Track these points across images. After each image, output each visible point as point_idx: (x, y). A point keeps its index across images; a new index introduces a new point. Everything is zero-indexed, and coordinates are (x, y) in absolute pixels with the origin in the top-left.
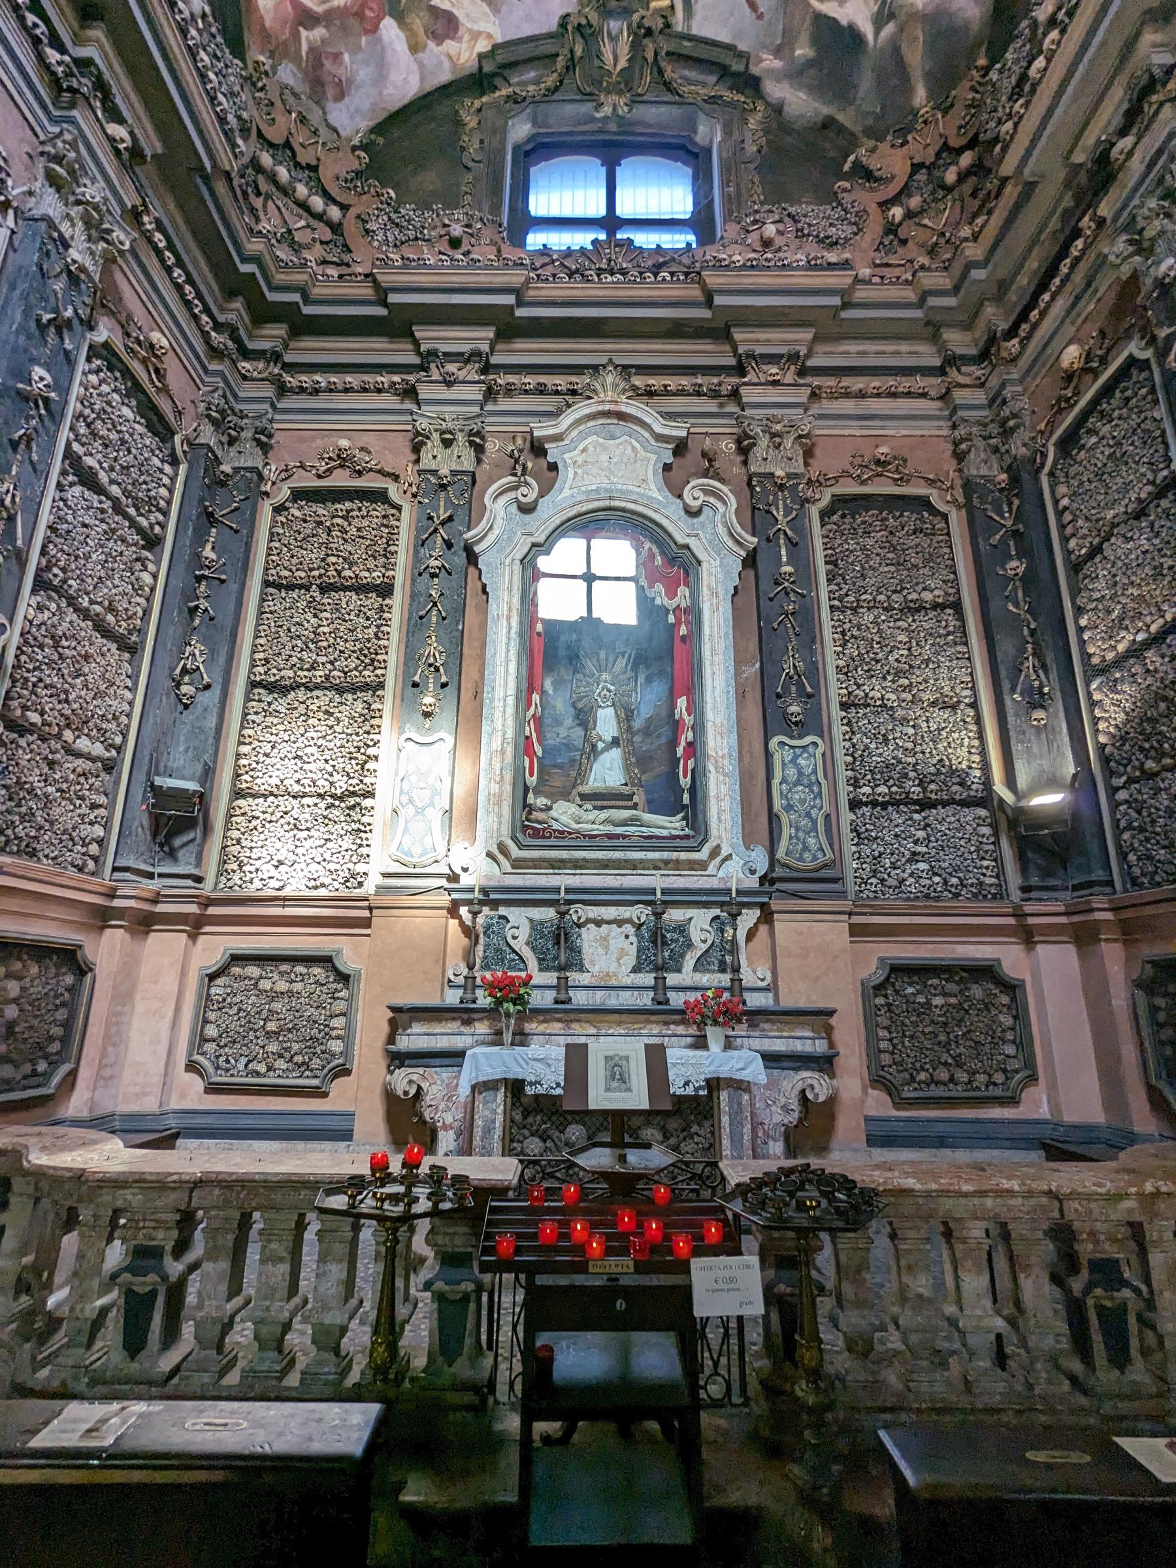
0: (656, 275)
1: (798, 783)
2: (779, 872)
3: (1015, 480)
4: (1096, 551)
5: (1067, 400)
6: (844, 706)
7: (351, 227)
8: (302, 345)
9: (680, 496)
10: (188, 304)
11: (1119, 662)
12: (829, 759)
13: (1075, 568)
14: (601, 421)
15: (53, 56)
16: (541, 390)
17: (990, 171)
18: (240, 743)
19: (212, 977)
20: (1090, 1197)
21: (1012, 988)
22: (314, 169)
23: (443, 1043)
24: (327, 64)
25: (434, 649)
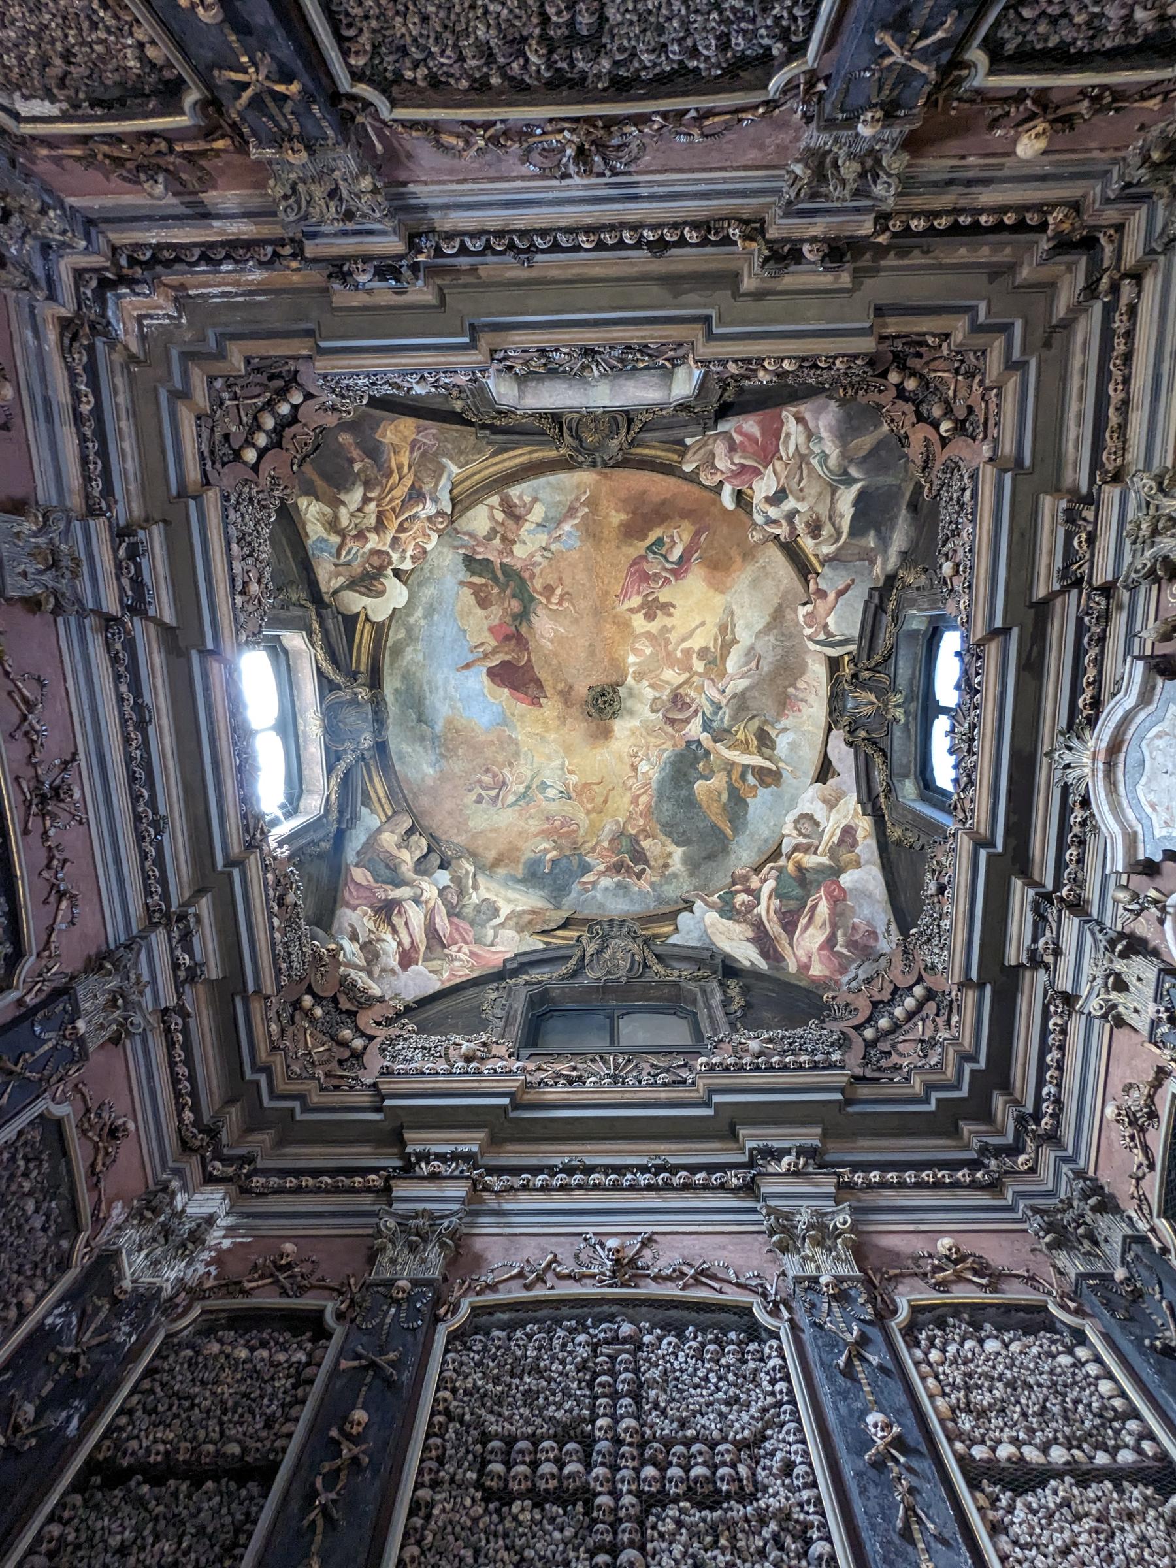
0: (977, 692)
5: (1095, 100)
8: (1018, 1084)
14: (1120, 775)
24: (857, 937)
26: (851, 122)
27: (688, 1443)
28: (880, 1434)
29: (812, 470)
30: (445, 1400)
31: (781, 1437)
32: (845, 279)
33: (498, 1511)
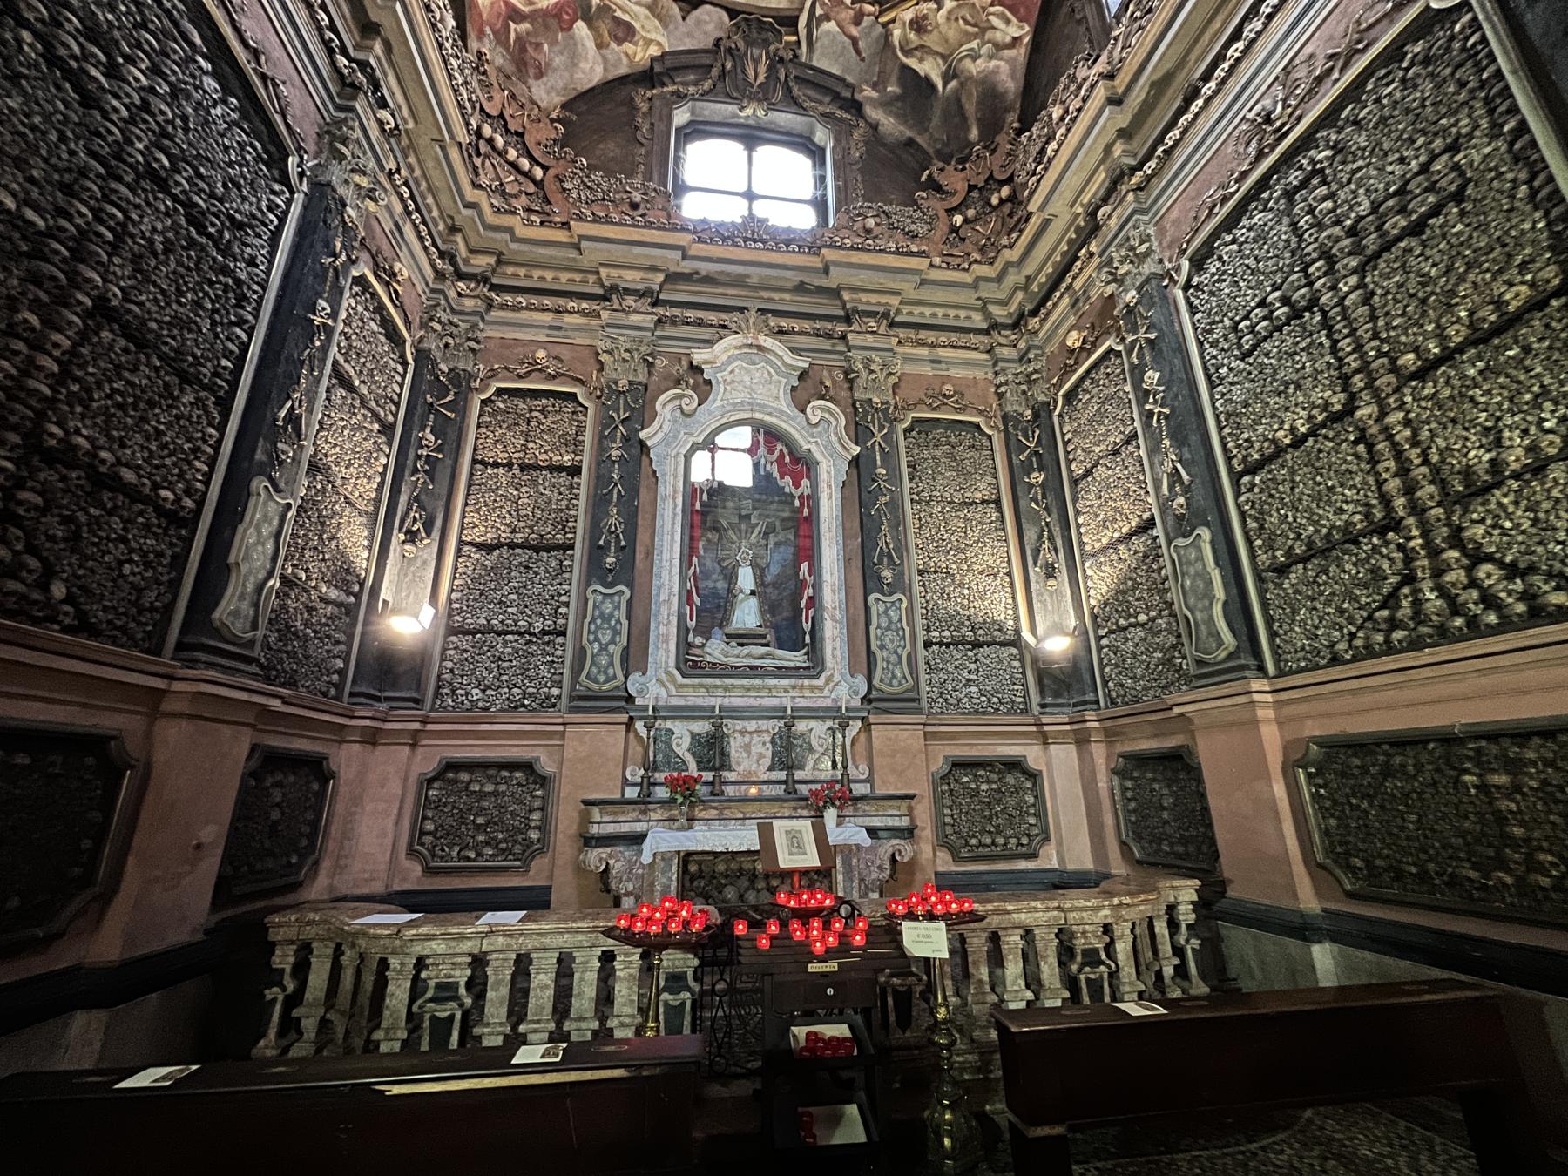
1: (888, 628)
2: (874, 694)
3: (1036, 416)
4: (1088, 473)
6: (921, 572)
7: (550, 185)
9: (803, 411)
10: (421, 239)
11: (1103, 550)
12: (911, 610)
13: (1075, 482)
15: (342, 61)
16: (700, 323)
17: (1020, 203)
19: (430, 781)
20: (1083, 909)
21: (1033, 776)
22: (521, 135)
23: (625, 828)
24: (530, 50)
25: (614, 519)
26: (1139, 291)
29: (970, 37)
32: (1080, 210)
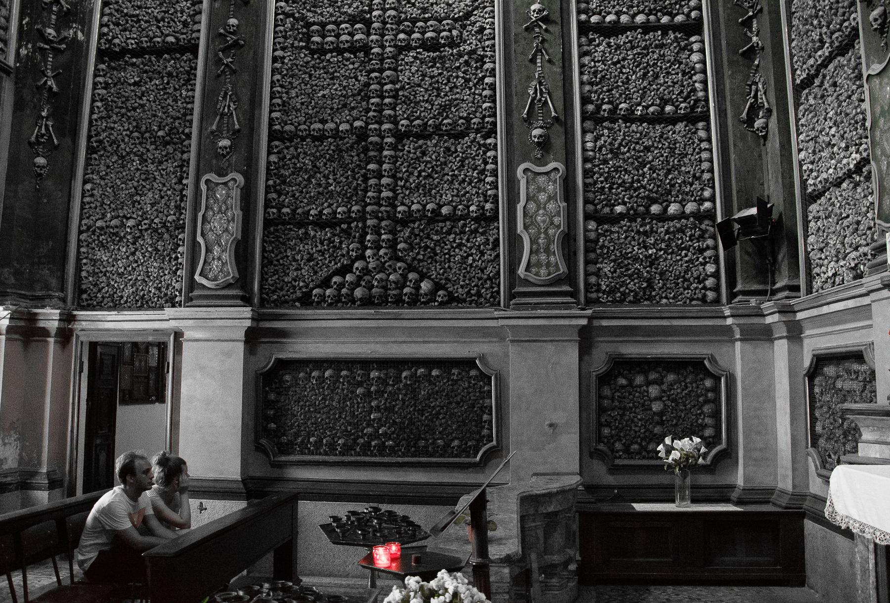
18: (800, 150)
27: (426, 20)
28: (535, 15)
30: (281, 7)
31: (482, 14)
33: (319, 58)
